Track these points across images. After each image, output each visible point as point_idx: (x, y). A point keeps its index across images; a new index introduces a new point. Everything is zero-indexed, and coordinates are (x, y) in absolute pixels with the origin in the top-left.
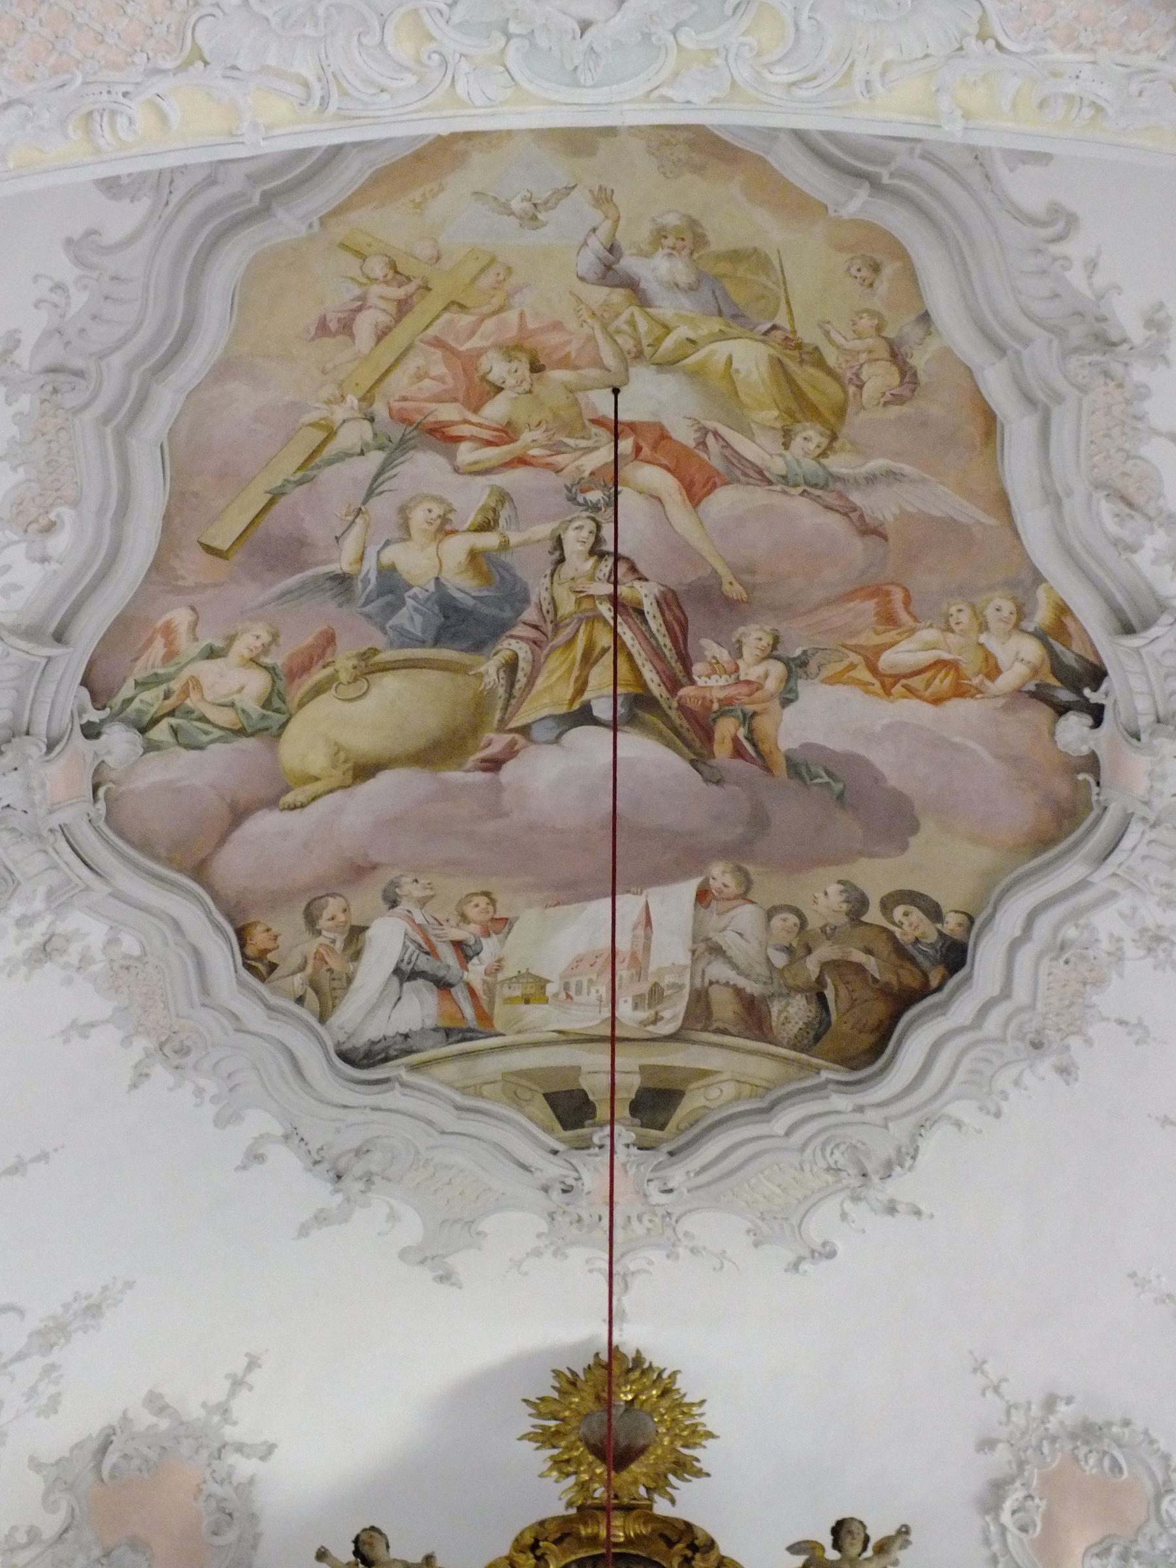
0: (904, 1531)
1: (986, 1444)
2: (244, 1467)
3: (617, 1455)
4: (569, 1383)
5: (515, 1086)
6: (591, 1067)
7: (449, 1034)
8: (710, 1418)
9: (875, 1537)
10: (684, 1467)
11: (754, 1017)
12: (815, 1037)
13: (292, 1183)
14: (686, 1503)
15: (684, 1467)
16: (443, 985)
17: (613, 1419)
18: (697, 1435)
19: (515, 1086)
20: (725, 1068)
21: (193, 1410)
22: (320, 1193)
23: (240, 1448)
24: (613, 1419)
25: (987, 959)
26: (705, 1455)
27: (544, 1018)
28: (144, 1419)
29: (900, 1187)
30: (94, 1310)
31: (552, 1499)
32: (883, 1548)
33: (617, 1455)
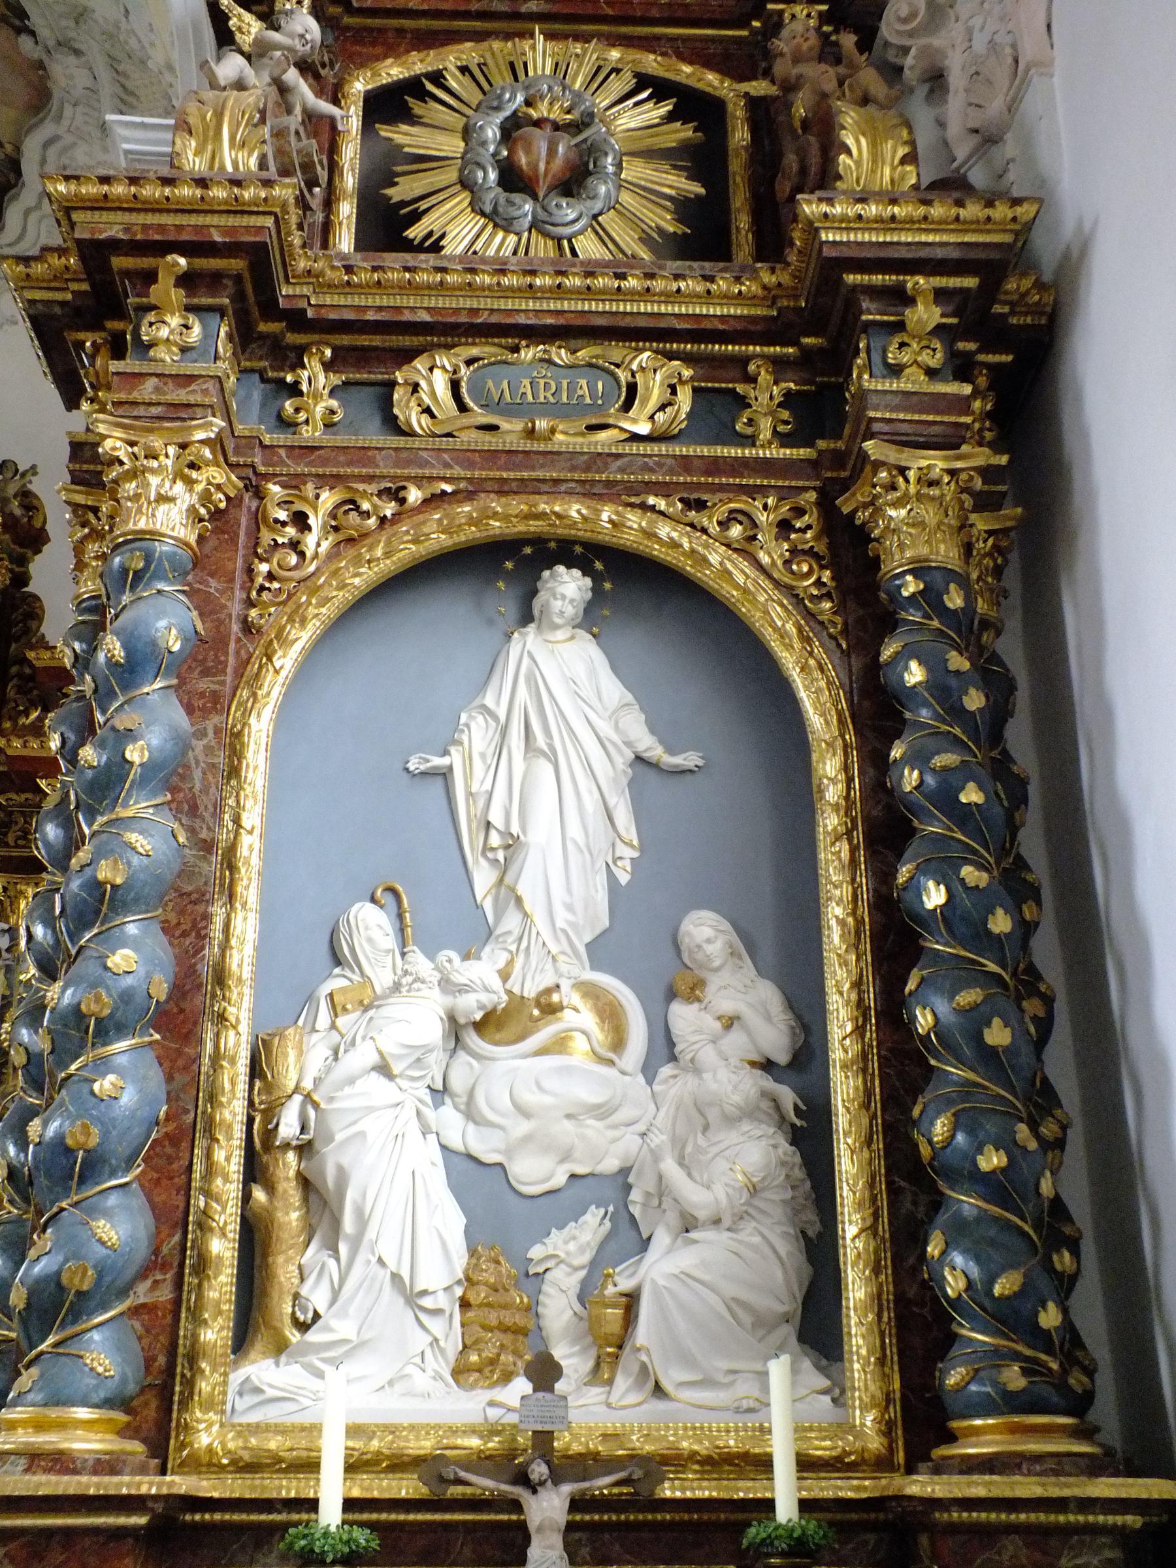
0: (34, 467)
9: (21, 469)
32: (23, 475)
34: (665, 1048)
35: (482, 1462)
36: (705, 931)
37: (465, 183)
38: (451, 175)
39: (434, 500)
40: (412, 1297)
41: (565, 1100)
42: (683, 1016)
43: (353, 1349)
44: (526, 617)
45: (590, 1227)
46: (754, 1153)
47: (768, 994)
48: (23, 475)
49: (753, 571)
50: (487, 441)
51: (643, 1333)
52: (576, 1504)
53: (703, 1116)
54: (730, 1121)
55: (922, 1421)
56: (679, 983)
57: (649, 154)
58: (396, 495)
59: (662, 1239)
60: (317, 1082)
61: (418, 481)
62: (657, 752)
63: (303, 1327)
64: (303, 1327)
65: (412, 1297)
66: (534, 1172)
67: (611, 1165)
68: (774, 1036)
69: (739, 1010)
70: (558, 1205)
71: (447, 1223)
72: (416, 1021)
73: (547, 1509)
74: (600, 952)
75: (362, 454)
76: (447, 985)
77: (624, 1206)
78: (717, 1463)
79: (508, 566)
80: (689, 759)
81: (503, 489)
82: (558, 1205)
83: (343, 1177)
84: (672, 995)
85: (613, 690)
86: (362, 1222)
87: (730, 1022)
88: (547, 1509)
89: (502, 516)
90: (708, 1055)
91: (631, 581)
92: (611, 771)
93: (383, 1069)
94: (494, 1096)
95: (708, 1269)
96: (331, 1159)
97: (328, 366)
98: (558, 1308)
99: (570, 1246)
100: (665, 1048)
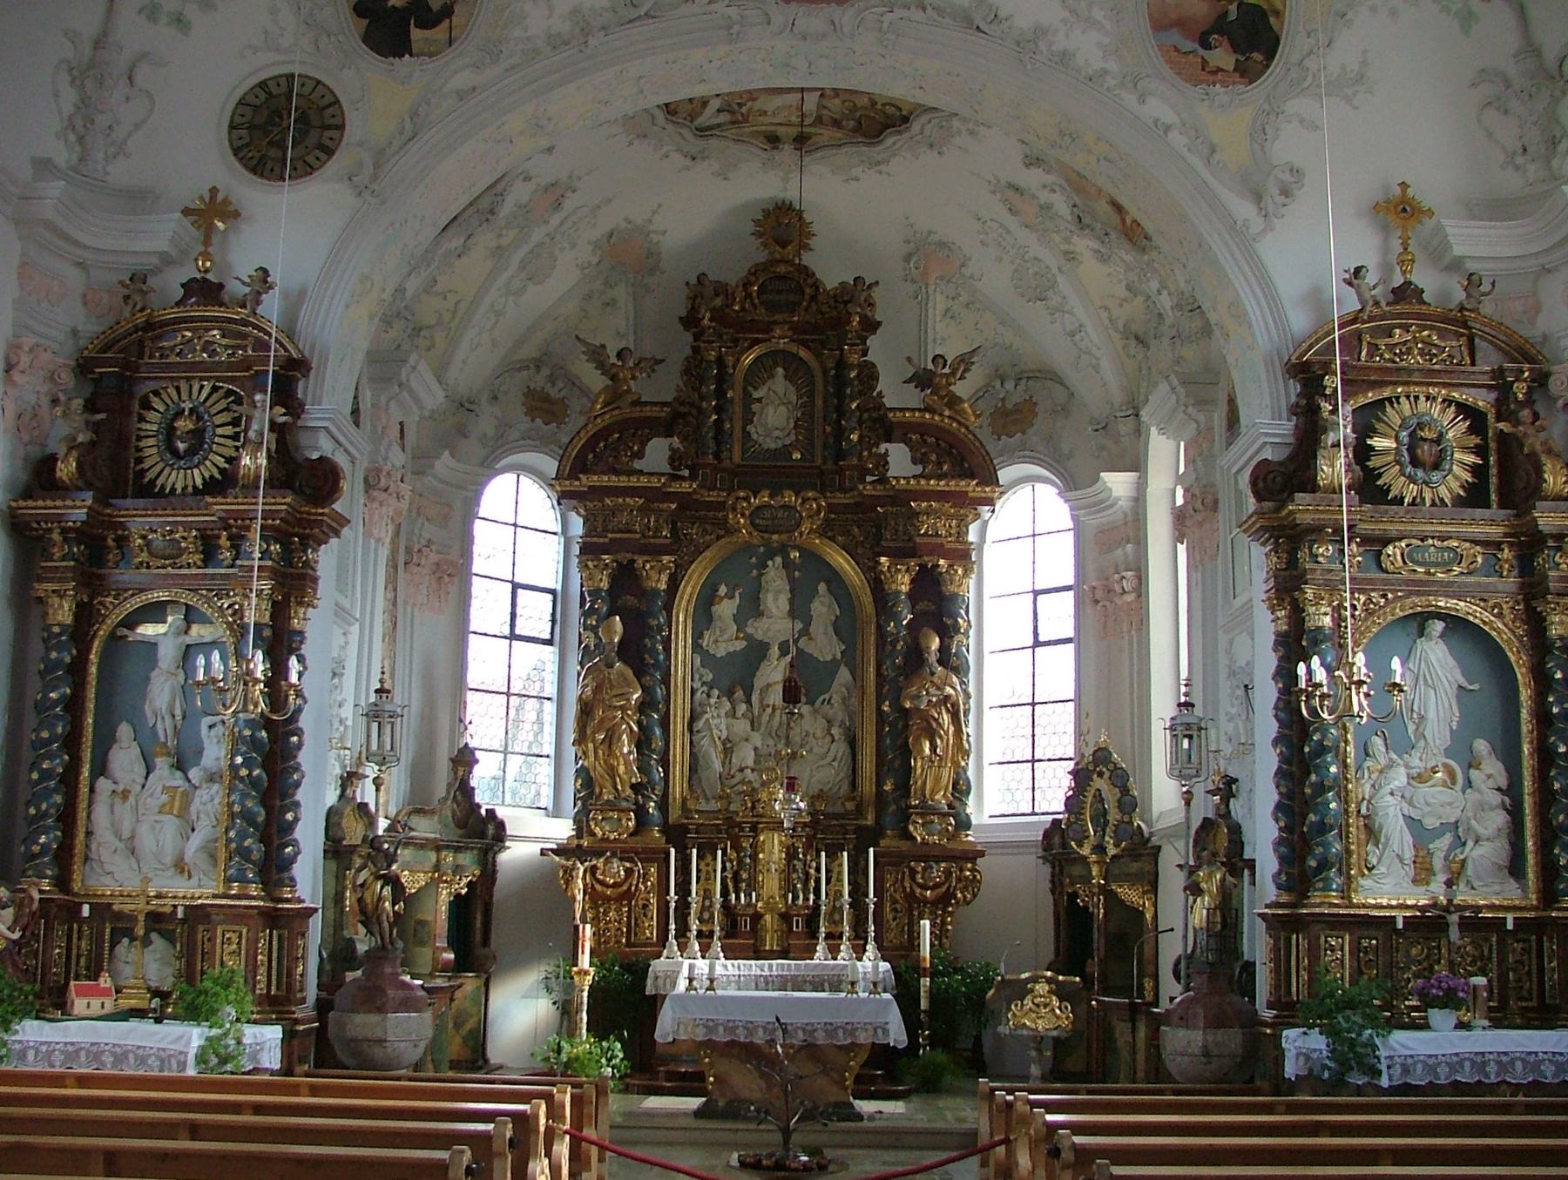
1: (908, 242)
2: (655, 238)
3: (784, 245)
4: (767, 213)
5: (755, 134)
6: (781, 131)
7: (734, 123)
8: (815, 228)
10: (807, 248)
11: (836, 123)
12: (858, 129)
13: (678, 160)
14: (808, 259)
15: (807, 248)
16: (733, 113)
17: (783, 225)
18: (811, 235)
19: (755, 134)
20: (826, 134)
21: (639, 222)
22: (688, 162)
23: (655, 232)
24: (783, 225)
25: (916, 126)
26: (812, 242)
27: (767, 120)
28: (623, 225)
29: (882, 167)
30: (609, 201)
31: (761, 256)
32: (870, 287)
33: (784, 245)
34: (1469, 783)
35: (1435, 905)
36: (1481, 746)
37: (1398, 462)
38: (1391, 458)
39: (1397, 598)
40: (1400, 858)
41: (1441, 802)
42: (1474, 773)
43: (1384, 875)
44: (1421, 635)
45: (1448, 839)
46: (1500, 819)
47: (1500, 766)
48: (870, 287)
49: (1505, 632)
50: (1412, 576)
51: (1470, 871)
52: (1461, 918)
53: (1481, 806)
54: (1492, 809)
55: (1549, 896)
56: (1472, 764)
57: (1464, 448)
58: (1385, 596)
59: (1470, 844)
60: (1371, 798)
61: (1392, 591)
62: (1465, 684)
63: (1370, 870)
64: (1370, 870)
65: (1401, 860)
66: (1431, 822)
67: (1452, 820)
68: (1503, 782)
69: (1491, 771)
70: (1438, 833)
71: (1408, 839)
72: (1399, 778)
73: (1454, 918)
74: (1448, 753)
75: (1371, 581)
76: (1407, 766)
77: (1458, 833)
78: (1491, 907)
79: (1419, 622)
80: (1475, 687)
81: (1418, 593)
82: (1438, 833)
83: (1381, 828)
84: (1470, 766)
85: (1451, 662)
86: (1388, 840)
87: (1489, 776)
88: (1454, 918)
89: (1418, 603)
90: (1483, 787)
91: (1457, 625)
92: (1452, 692)
93: (1392, 794)
94: (1419, 800)
95: (1486, 853)
96: (1378, 820)
97: (1358, 545)
98: (1438, 863)
99: (1441, 845)
100: (1469, 783)
